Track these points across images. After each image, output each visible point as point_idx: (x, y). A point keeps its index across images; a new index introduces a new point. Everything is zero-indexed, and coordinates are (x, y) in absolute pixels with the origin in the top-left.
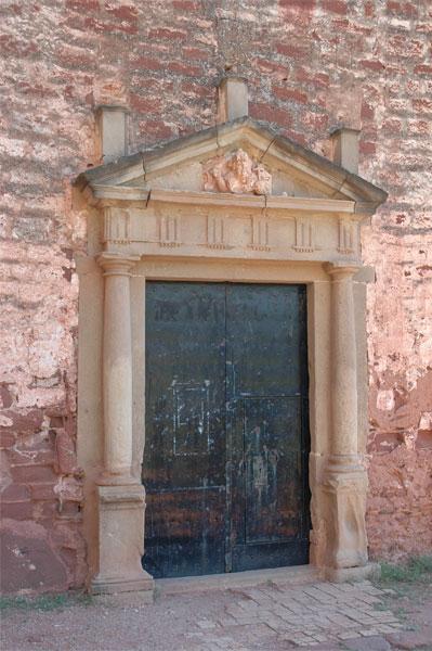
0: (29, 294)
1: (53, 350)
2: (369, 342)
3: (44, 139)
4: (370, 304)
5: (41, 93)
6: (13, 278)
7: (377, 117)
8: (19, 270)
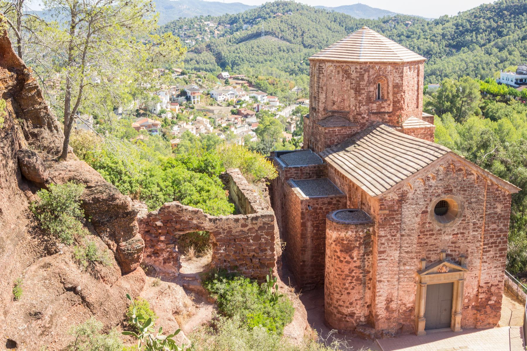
0: (409, 289)
1: (412, 298)
5: (413, 258)
8: (408, 286)
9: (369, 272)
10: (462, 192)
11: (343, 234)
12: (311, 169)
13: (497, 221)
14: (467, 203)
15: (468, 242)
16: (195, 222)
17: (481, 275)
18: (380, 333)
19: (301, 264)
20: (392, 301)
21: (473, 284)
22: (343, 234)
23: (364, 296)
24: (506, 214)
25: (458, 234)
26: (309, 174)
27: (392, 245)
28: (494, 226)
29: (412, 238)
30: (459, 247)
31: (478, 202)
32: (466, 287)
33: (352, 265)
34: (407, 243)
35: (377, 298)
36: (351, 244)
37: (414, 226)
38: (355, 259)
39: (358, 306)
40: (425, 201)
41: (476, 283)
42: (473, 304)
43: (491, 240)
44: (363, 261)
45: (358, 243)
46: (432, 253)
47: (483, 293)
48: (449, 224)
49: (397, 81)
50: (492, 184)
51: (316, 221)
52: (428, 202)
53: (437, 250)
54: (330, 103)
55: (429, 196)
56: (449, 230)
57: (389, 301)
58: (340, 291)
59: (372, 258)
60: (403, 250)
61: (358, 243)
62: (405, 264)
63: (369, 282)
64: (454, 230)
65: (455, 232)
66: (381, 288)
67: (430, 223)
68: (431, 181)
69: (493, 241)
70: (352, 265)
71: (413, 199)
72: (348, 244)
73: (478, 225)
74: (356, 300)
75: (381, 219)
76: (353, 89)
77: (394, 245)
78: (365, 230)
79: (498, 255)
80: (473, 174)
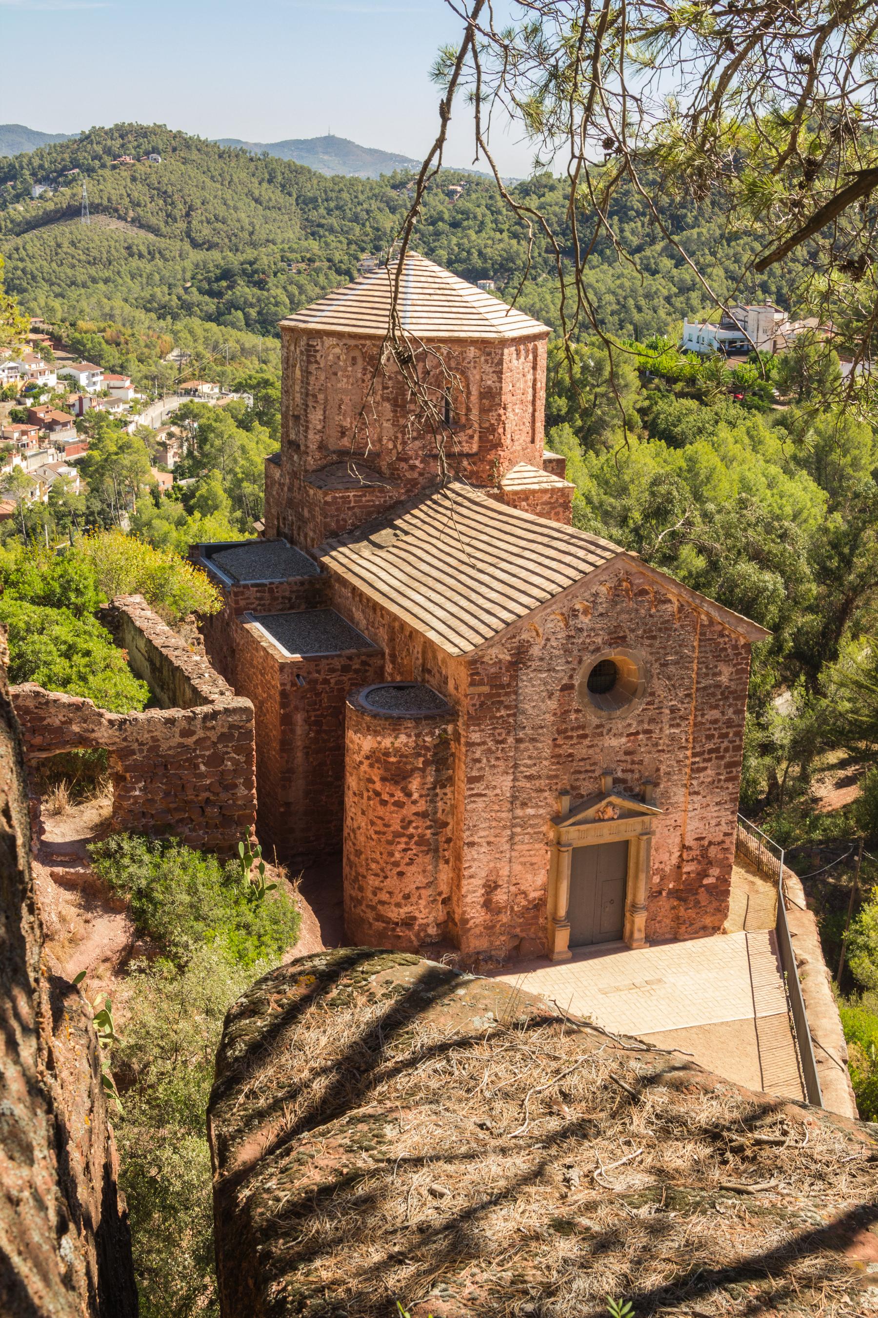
0: (534, 860)
1: (541, 878)
3: (541, 807)
5: (542, 791)
8: (532, 853)
9: (446, 824)
10: (647, 642)
11: (387, 742)
12: (295, 588)
13: (721, 703)
14: (657, 665)
15: (659, 751)
16: (75, 728)
17: (688, 821)
18: (473, 959)
19: (282, 810)
20: (497, 887)
21: (670, 841)
22: (387, 742)
23: (436, 878)
24: (741, 687)
25: (638, 733)
26: (290, 599)
27: (496, 763)
28: (715, 714)
29: (540, 745)
30: (641, 762)
31: (682, 661)
32: (656, 850)
33: (409, 810)
34: (530, 758)
35: (464, 882)
36: (406, 763)
37: (544, 720)
38: (416, 796)
39: (423, 902)
40: (568, 662)
41: (678, 840)
42: (671, 886)
43: (709, 746)
44: (432, 801)
45: (421, 759)
46: (582, 776)
47: (692, 860)
48: (618, 712)
49: (489, 383)
50: (711, 622)
51: (315, 710)
52: (574, 665)
53: (594, 771)
54: (334, 433)
55: (575, 653)
56: (620, 726)
57: (491, 887)
58: (382, 870)
59: (453, 792)
60: (522, 772)
61: (421, 759)
62: (524, 805)
63: (446, 846)
64: (630, 725)
65: (633, 730)
66: (474, 860)
67: (578, 711)
68: (582, 617)
69: (712, 746)
70: (409, 810)
71: (541, 659)
72: (399, 762)
73: (681, 713)
74: (418, 888)
75: (474, 705)
76: (388, 400)
77: (501, 763)
78: (437, 732)
79: (722, 777)
80: (670, 601)
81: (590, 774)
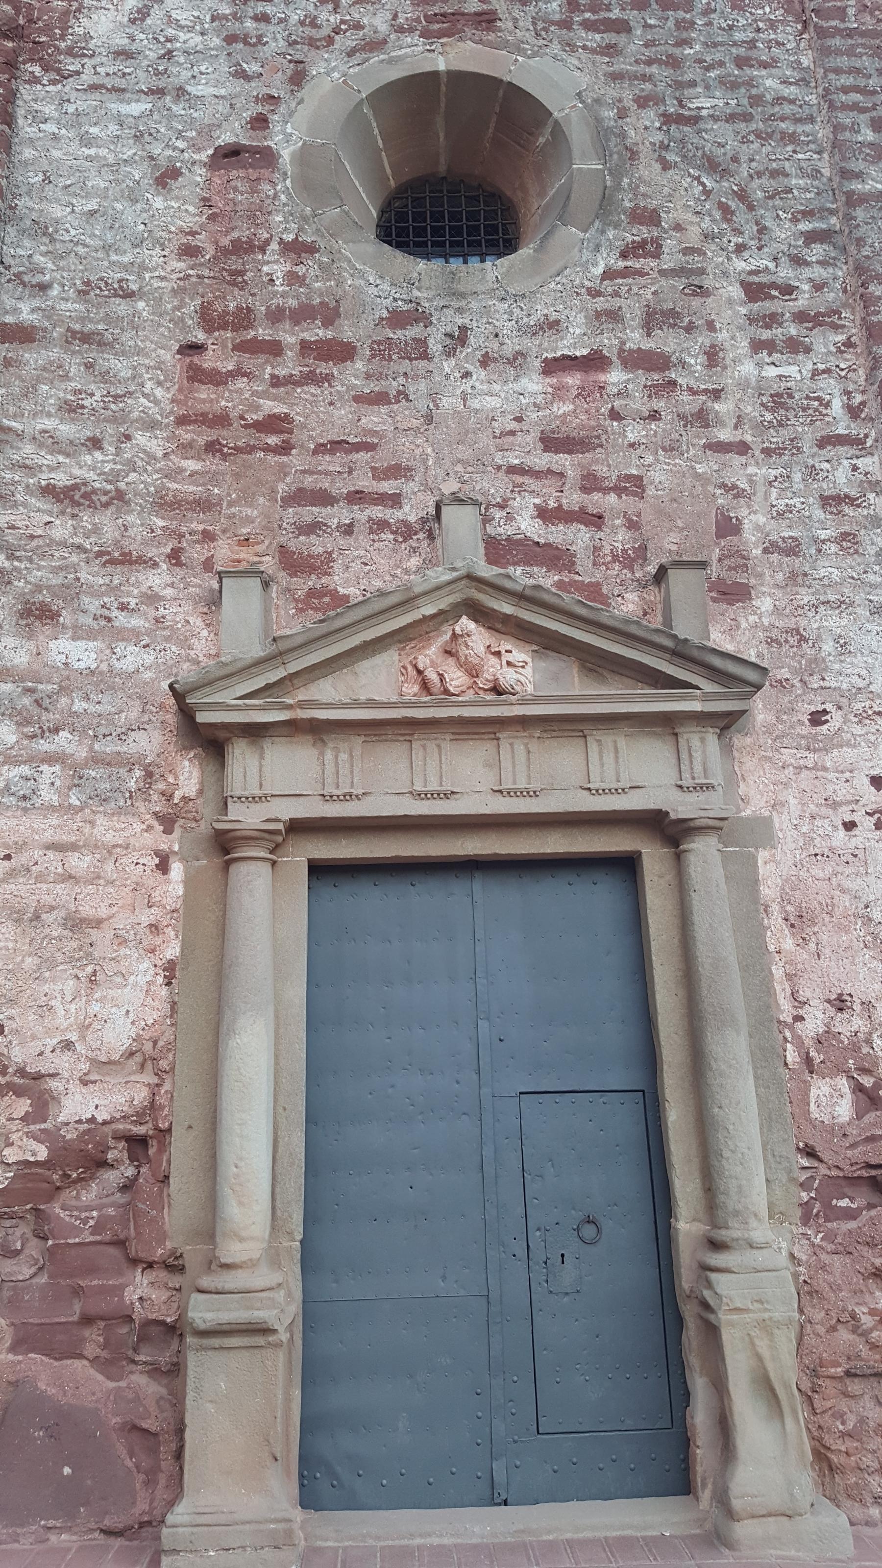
2: (778, 972)
3: (133, 636)
4: (768, 891)
5: (127, 560)
6: (69, 877)
7: (749, 535)
8: (79, 863)
10: (595, 39)
14: (650, 117)
29: (120, 367)
40: (241, 75)
53: (395, 500)
56: (507, 327)
60: (28, 468)
64: (553, 325)
73: (802, 302)
81: (377, 512)
